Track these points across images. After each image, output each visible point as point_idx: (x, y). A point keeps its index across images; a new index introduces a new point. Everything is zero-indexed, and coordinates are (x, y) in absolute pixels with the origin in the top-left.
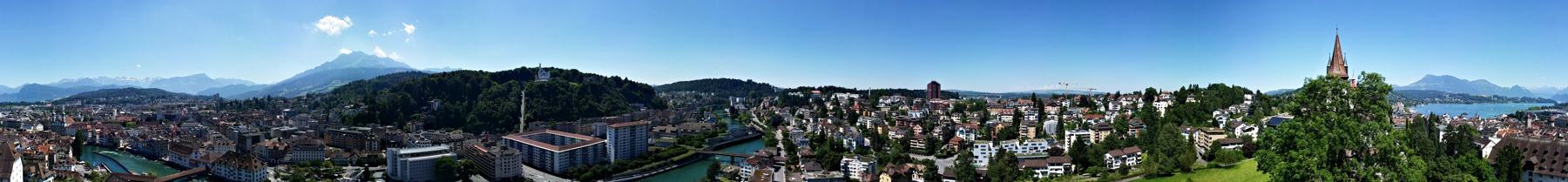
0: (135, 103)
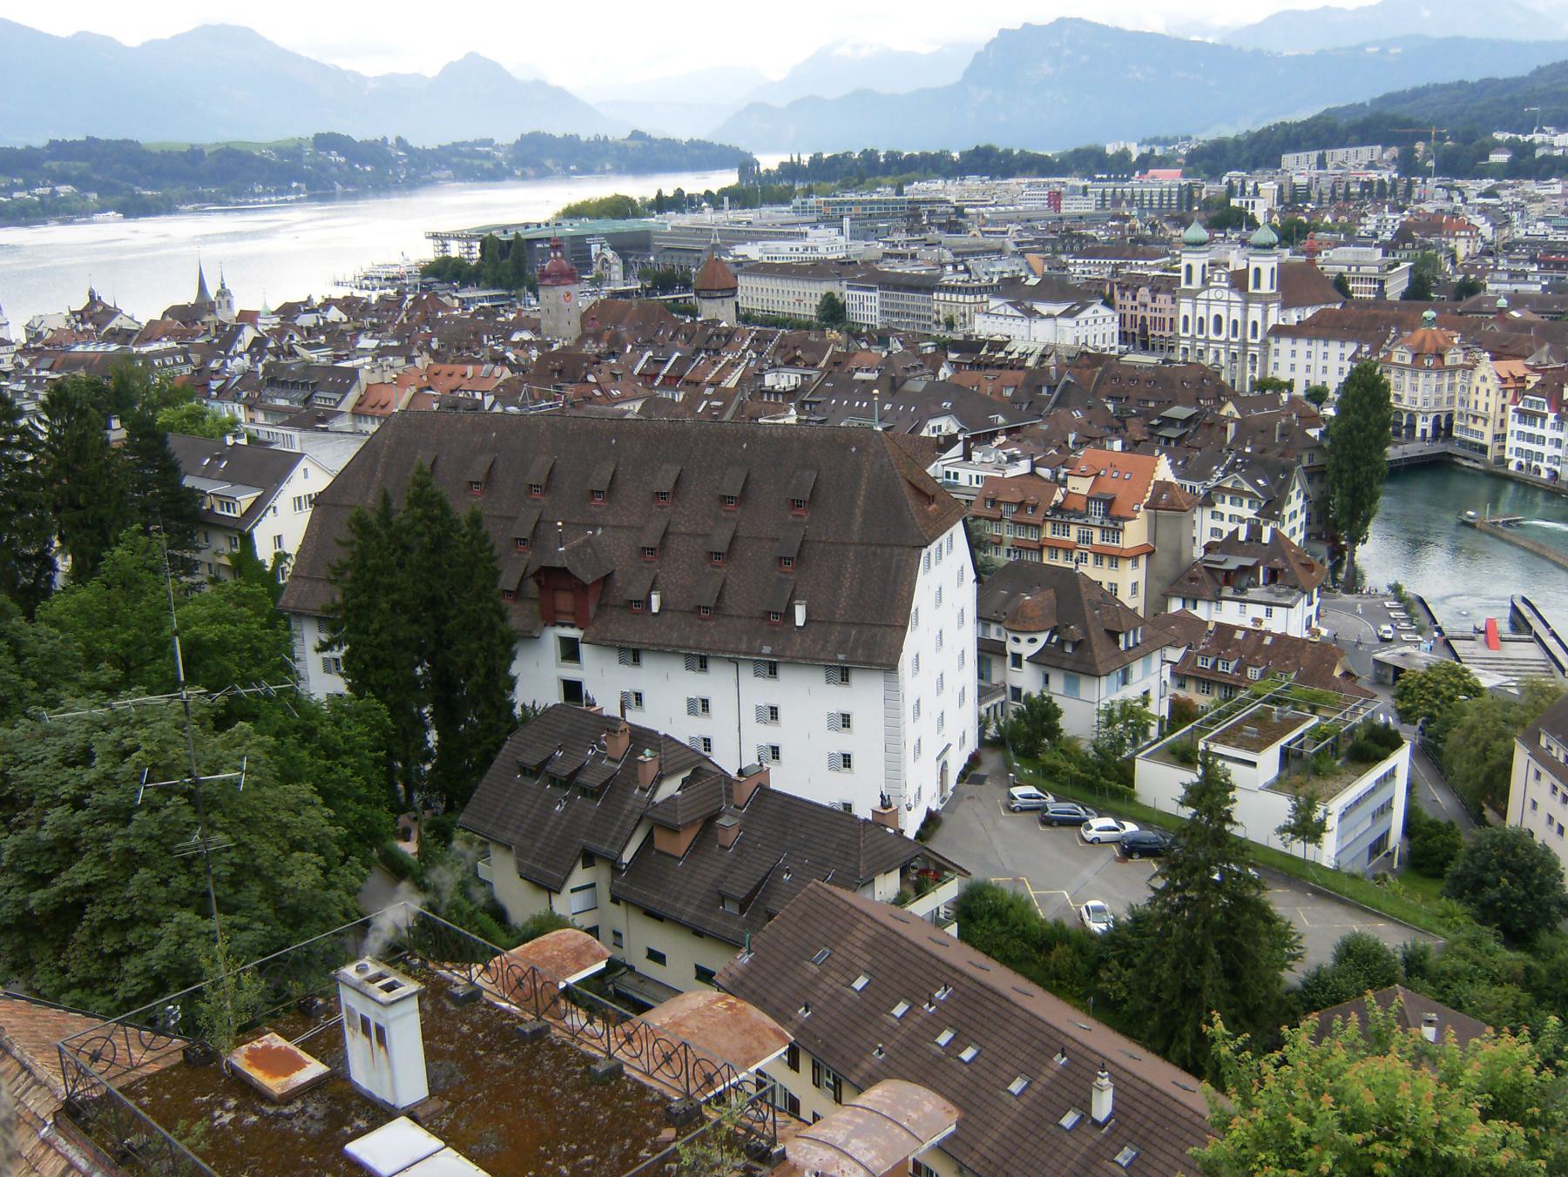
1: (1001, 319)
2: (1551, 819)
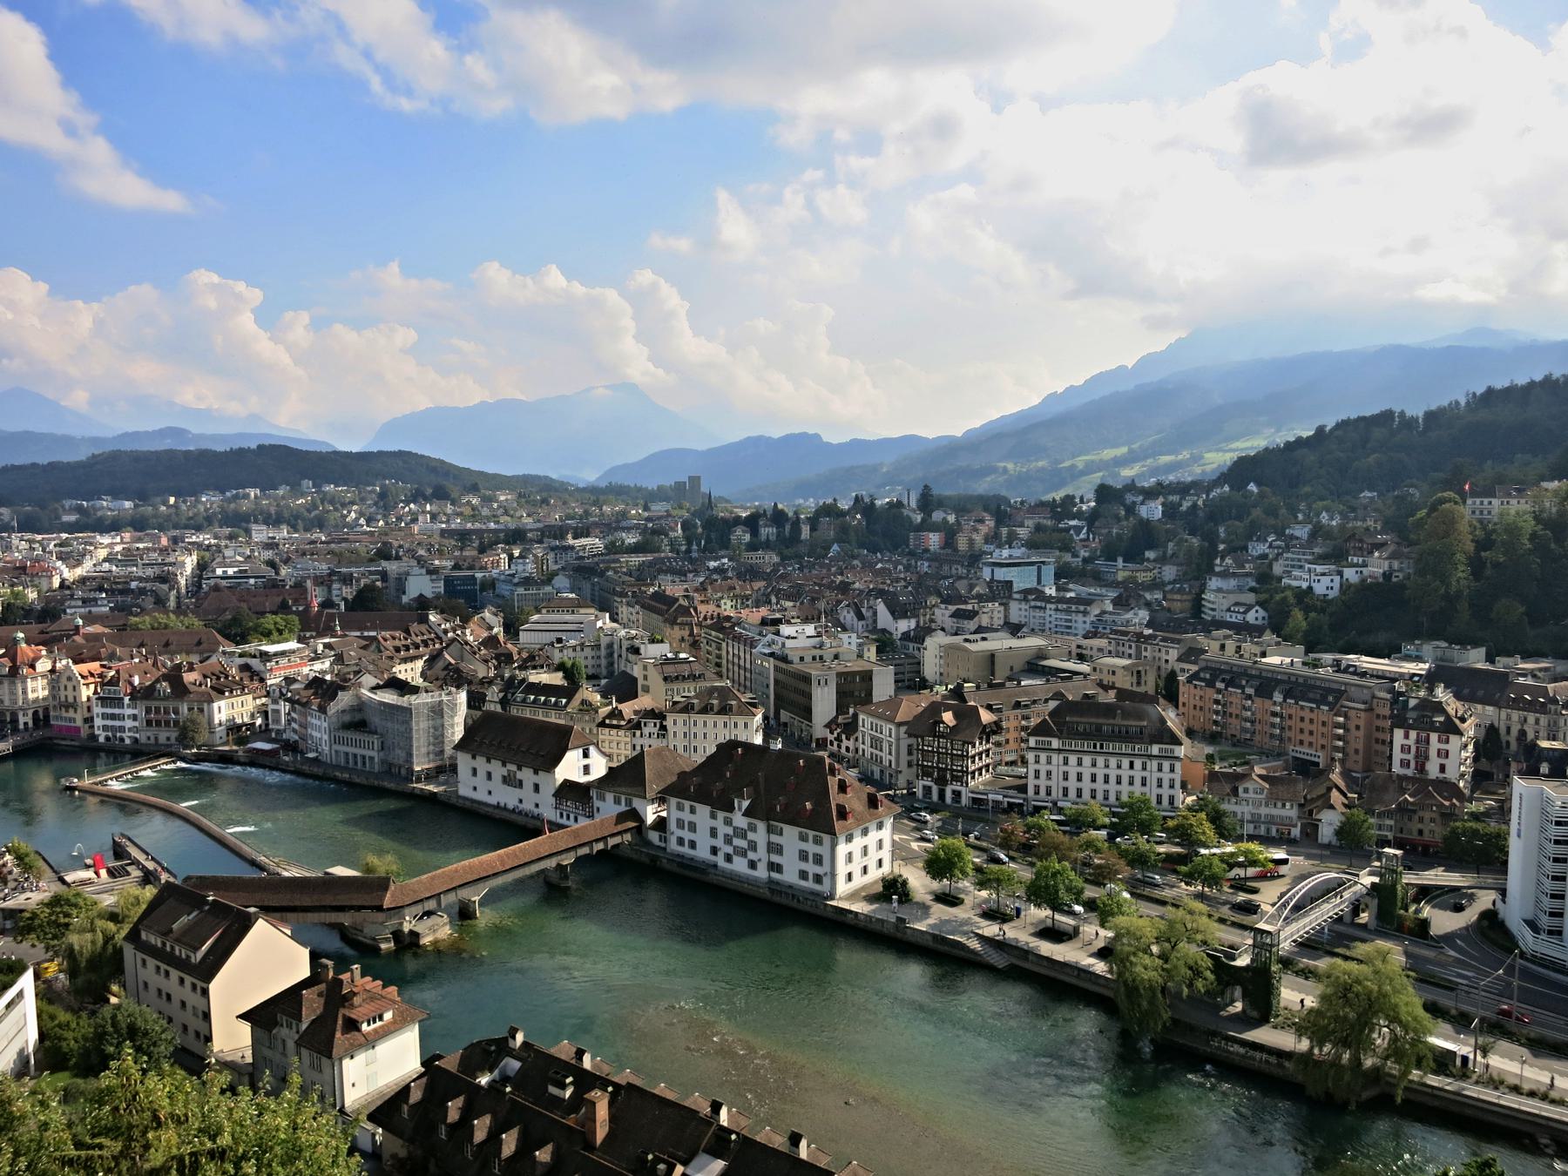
0: (293, 521)
2: (160, 991)
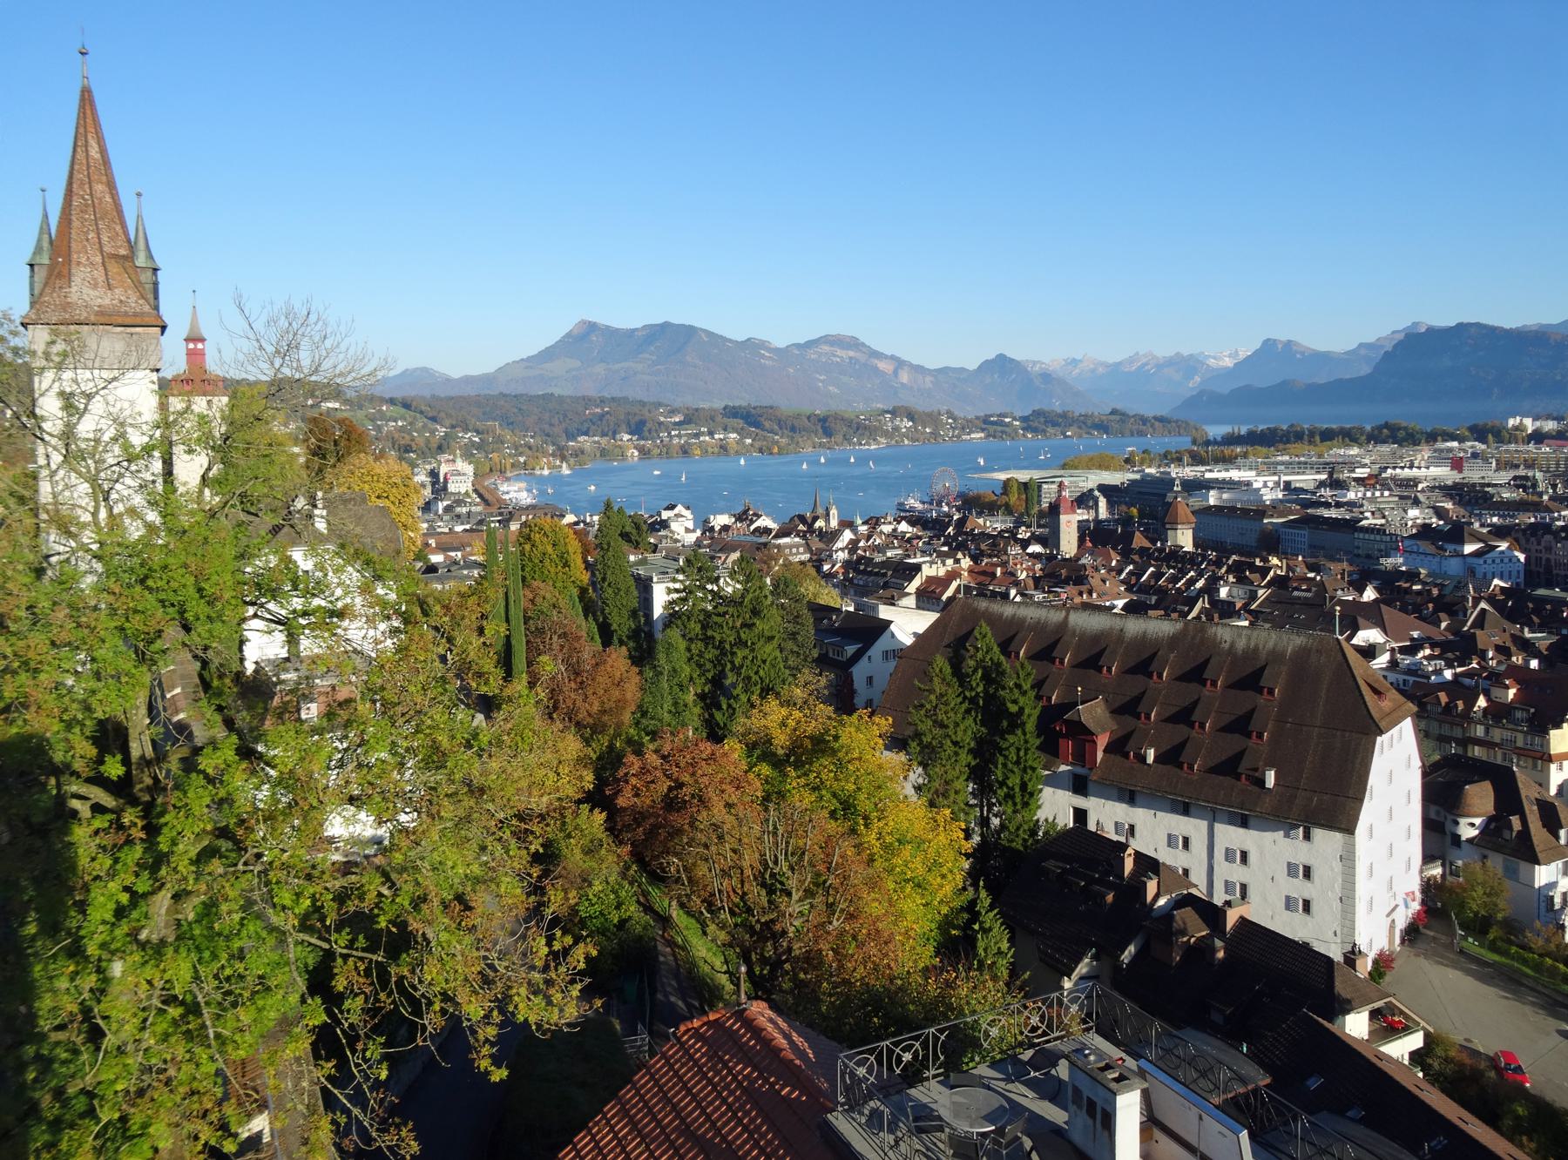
1: (1414, 556)
